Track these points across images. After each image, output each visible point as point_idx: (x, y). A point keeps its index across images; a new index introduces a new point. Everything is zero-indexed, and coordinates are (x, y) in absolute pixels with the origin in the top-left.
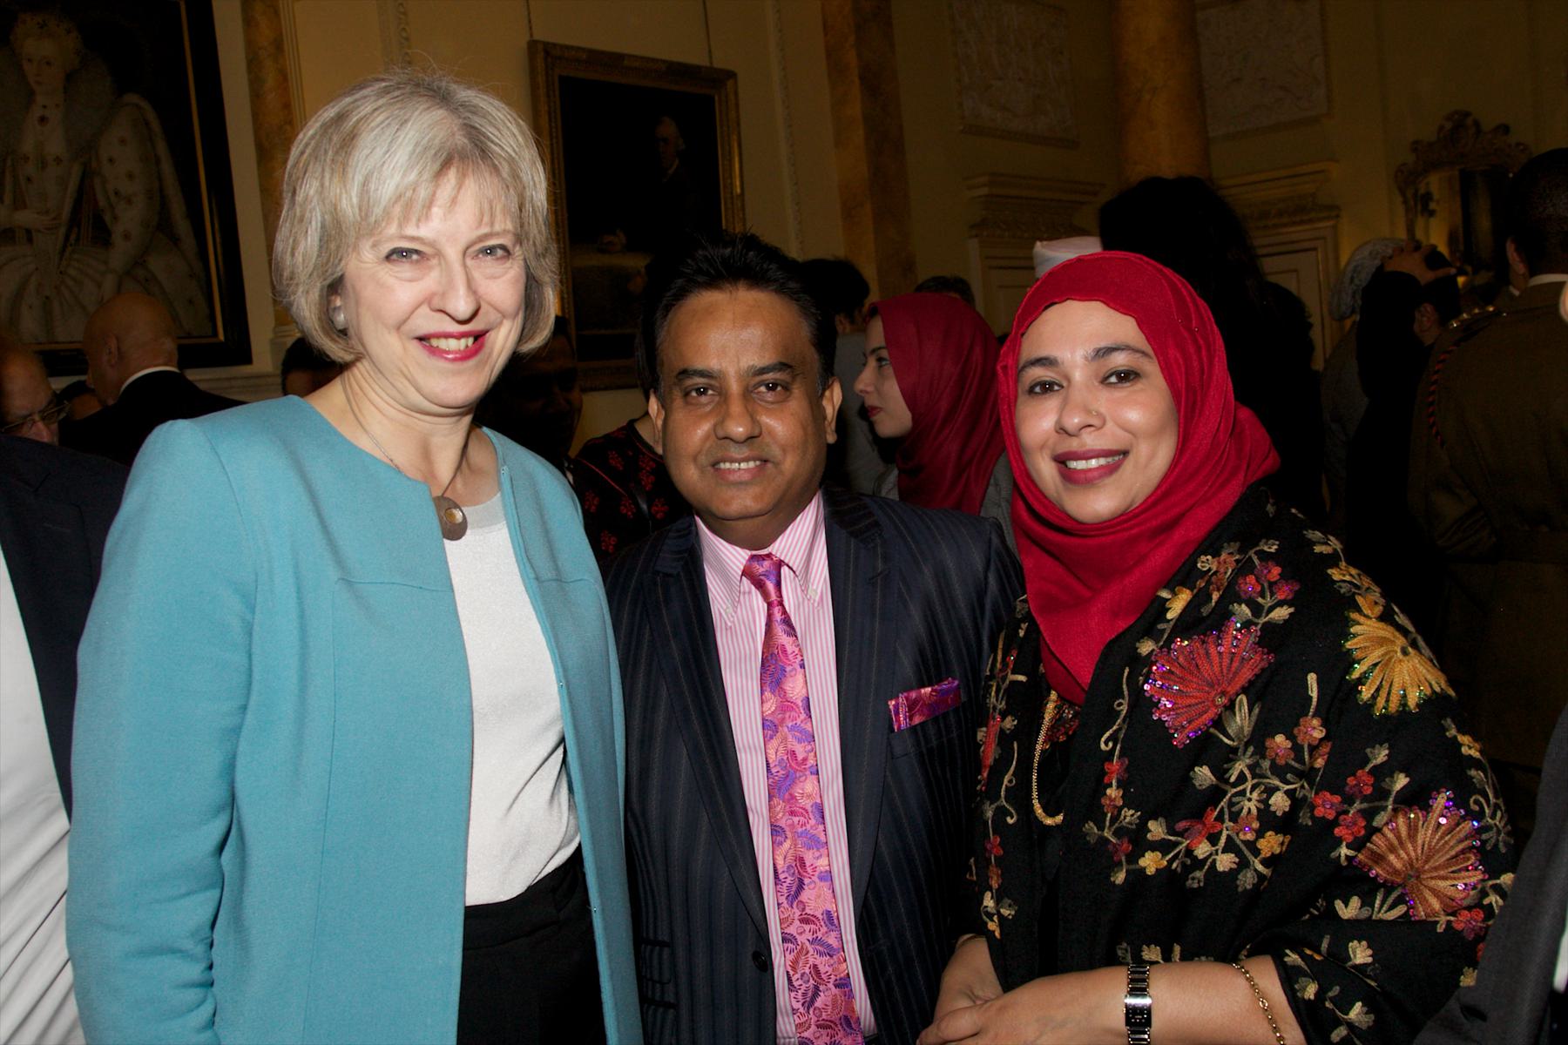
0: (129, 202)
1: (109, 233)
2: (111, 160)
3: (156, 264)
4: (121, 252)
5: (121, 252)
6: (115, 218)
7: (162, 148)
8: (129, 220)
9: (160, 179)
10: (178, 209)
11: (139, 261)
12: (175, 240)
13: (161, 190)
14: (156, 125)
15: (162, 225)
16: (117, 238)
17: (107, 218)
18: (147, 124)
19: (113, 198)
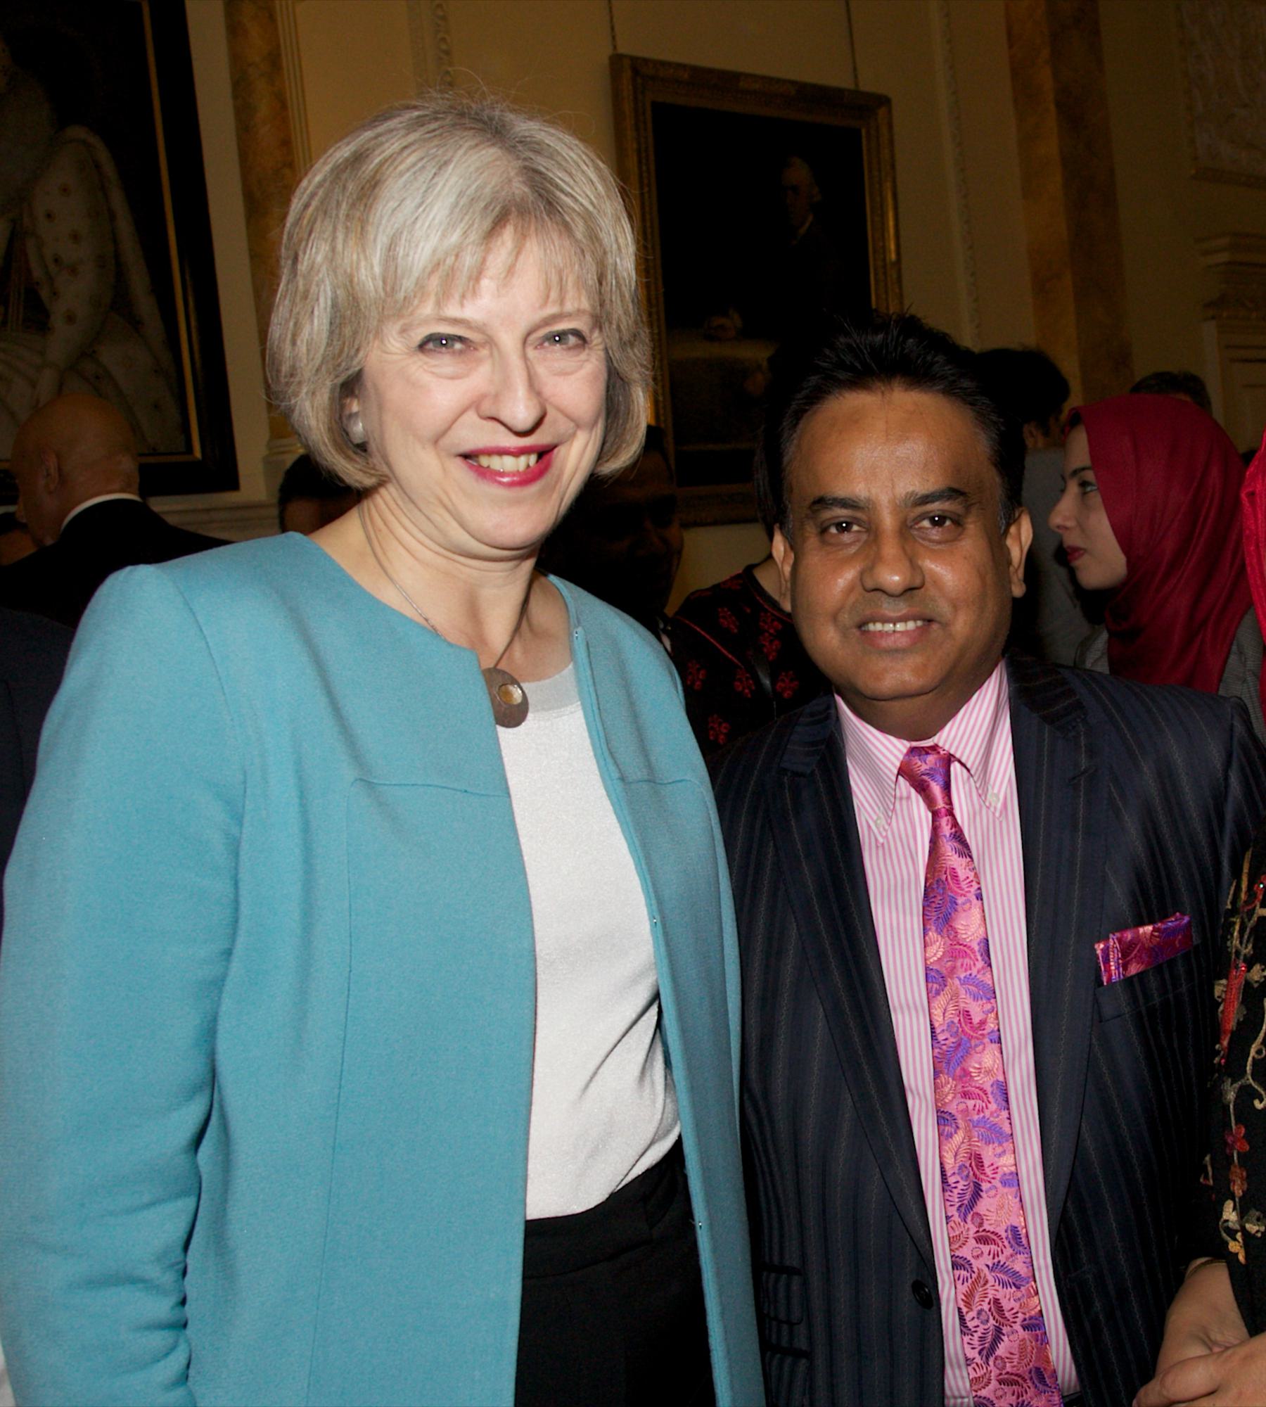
0: (73, 271)
1: (47, 314)
2: (49, 216)
3: (110, 356)
4: (63, 339)
5: (63, 339)
6: (55, 294)
7: (118, 200)
8: (74, 296)
9: (115, 241)
10: (139, 281)
11: (87, 352)
12: (136, 324)
13: (117, 256)
14: (109, 169)
15: (118, 303)
16: (57, 321)
17: (44, 294)
18: (98, 166)
19: (52, 268)
